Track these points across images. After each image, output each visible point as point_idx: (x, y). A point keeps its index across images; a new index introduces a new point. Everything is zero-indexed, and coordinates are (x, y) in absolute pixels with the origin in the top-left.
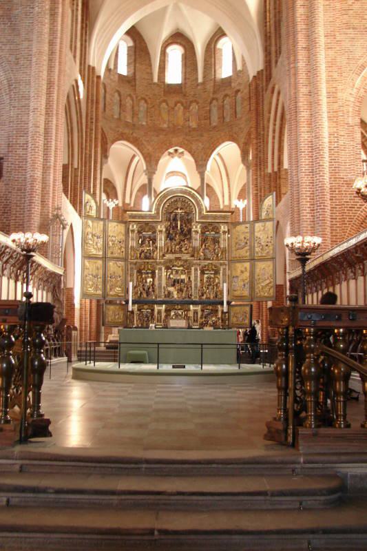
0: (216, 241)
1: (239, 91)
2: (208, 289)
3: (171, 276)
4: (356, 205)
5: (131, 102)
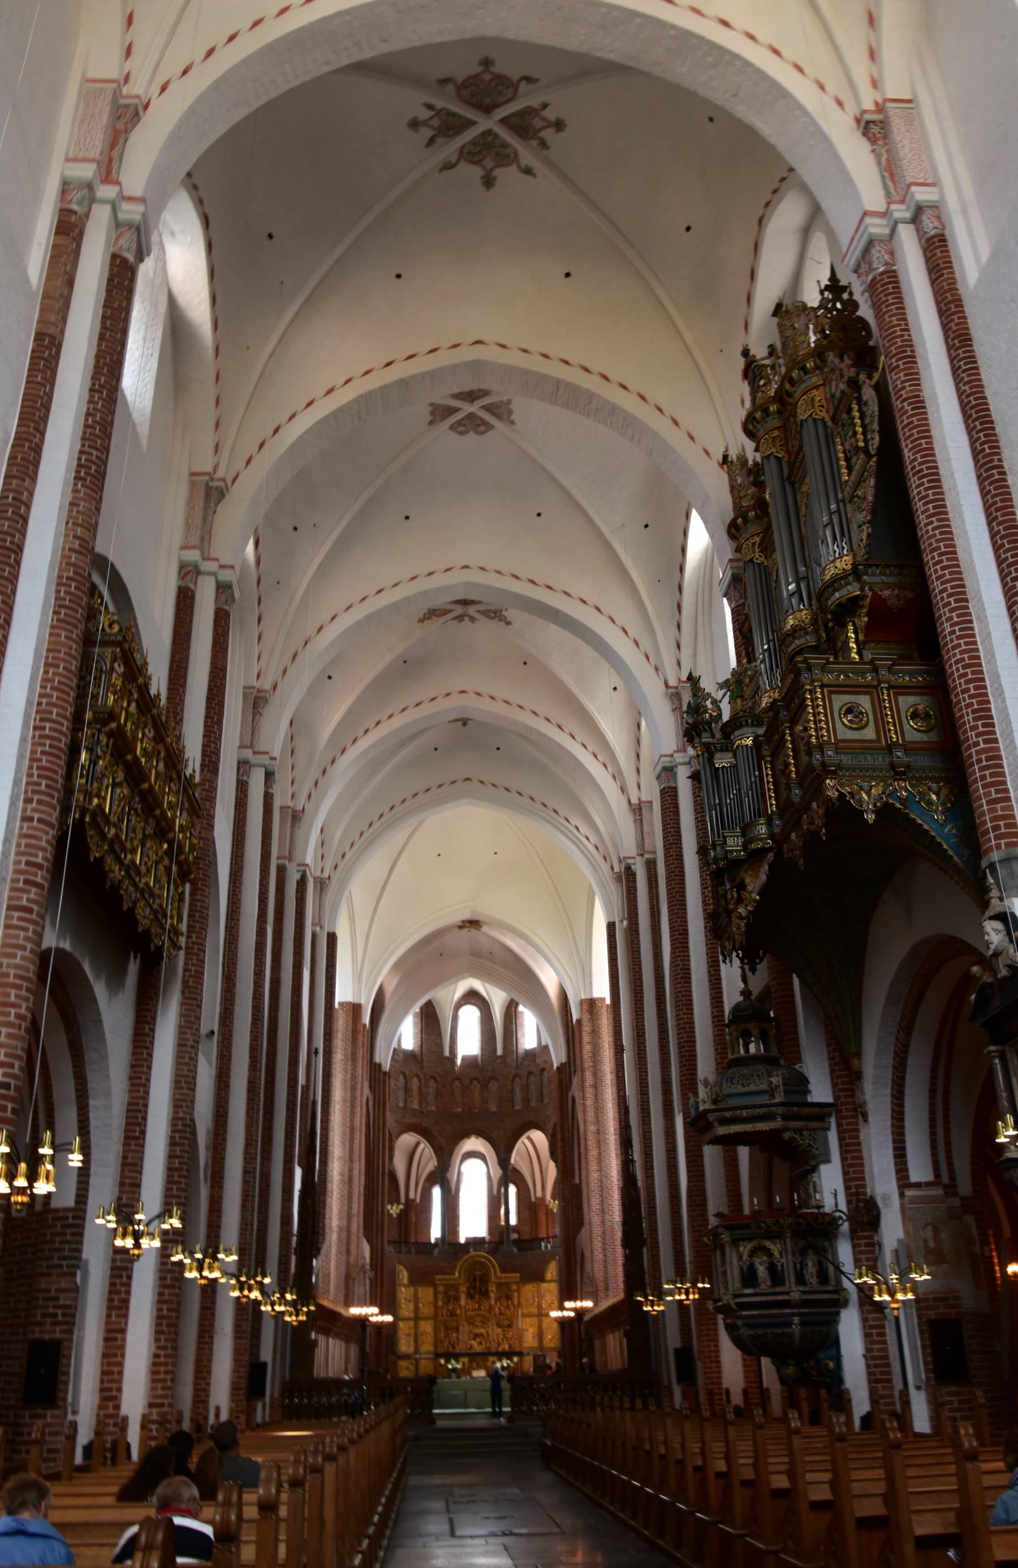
0: (509, 1298)
1: (543, 1069)
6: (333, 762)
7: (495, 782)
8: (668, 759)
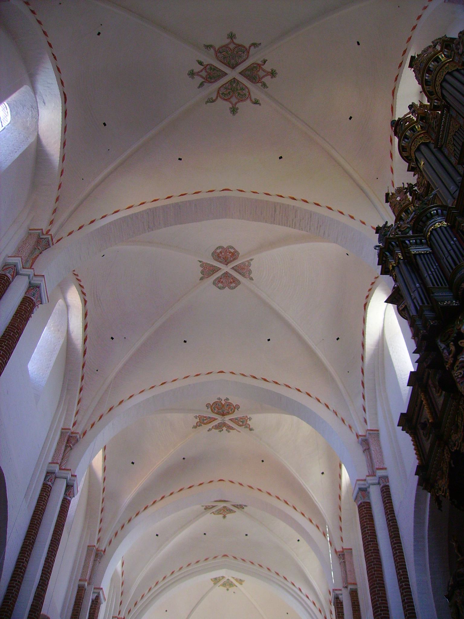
6: (130, 521)
7: (244, 558)
8: (363, 482)
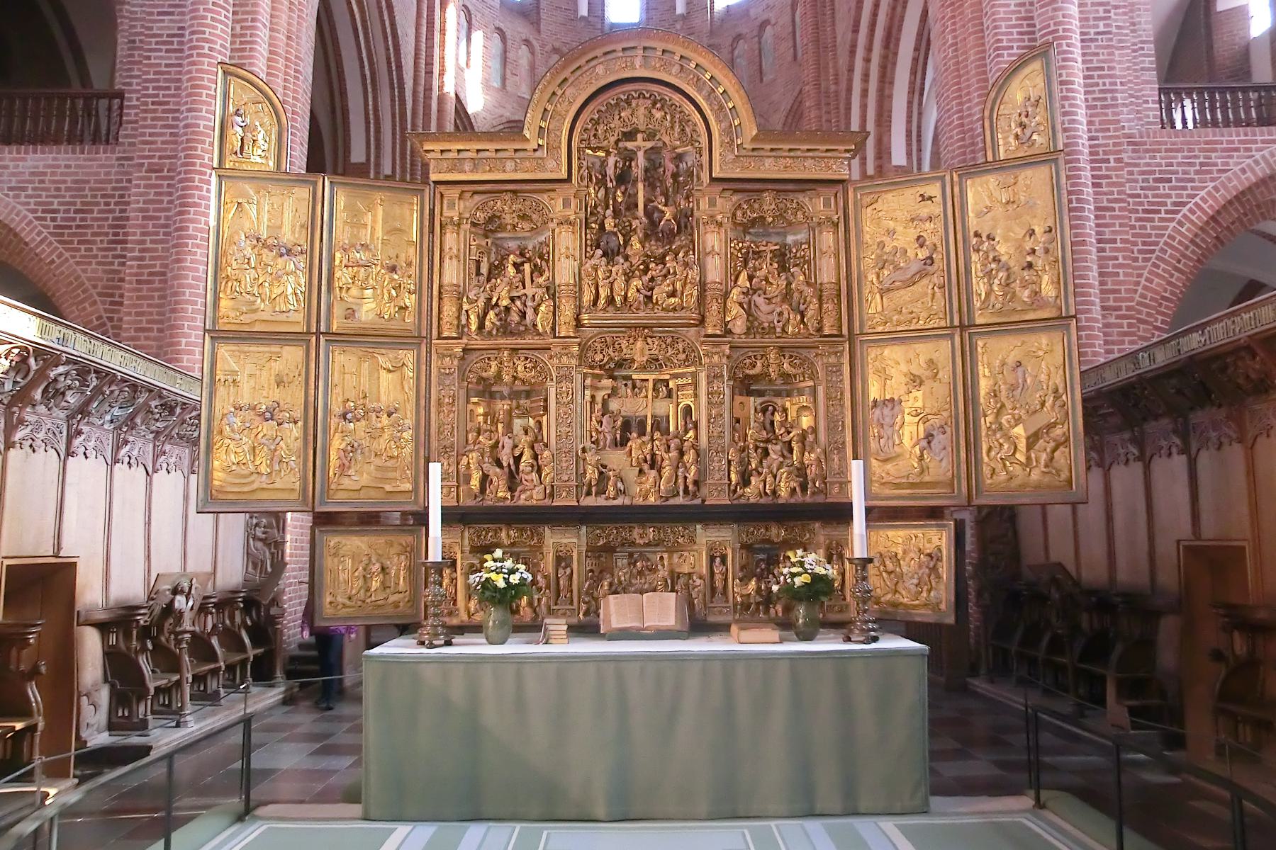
1: (764, 25)
2: (766, 453)
3: (614, 405)
4: (1165, 204)
5: (529, 55)
